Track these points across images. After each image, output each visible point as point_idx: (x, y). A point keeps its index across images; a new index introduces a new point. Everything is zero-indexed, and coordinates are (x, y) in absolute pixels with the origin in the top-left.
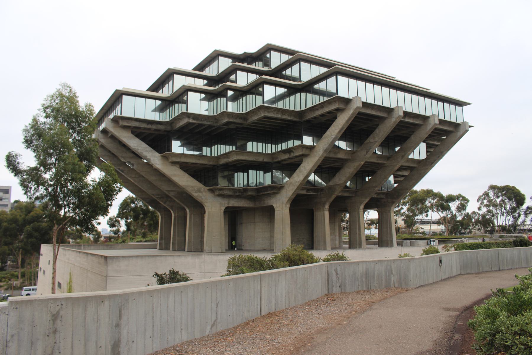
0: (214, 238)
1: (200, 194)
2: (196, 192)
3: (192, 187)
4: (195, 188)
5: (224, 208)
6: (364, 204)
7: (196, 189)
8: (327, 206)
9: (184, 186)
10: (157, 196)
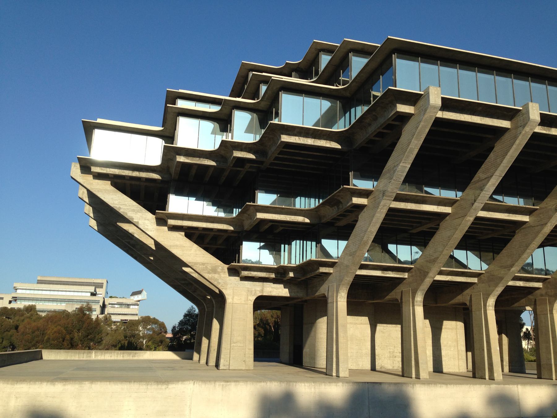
0: (234, 345)
1: (216, 276)
2: (209, 273)
3: (203, 264)
4: (208, 267)
5: (254, 298)
6: (496, 297)
7: (209, 267)
8: (419, 298)
9: (190, 263)
10: (183, 282)
